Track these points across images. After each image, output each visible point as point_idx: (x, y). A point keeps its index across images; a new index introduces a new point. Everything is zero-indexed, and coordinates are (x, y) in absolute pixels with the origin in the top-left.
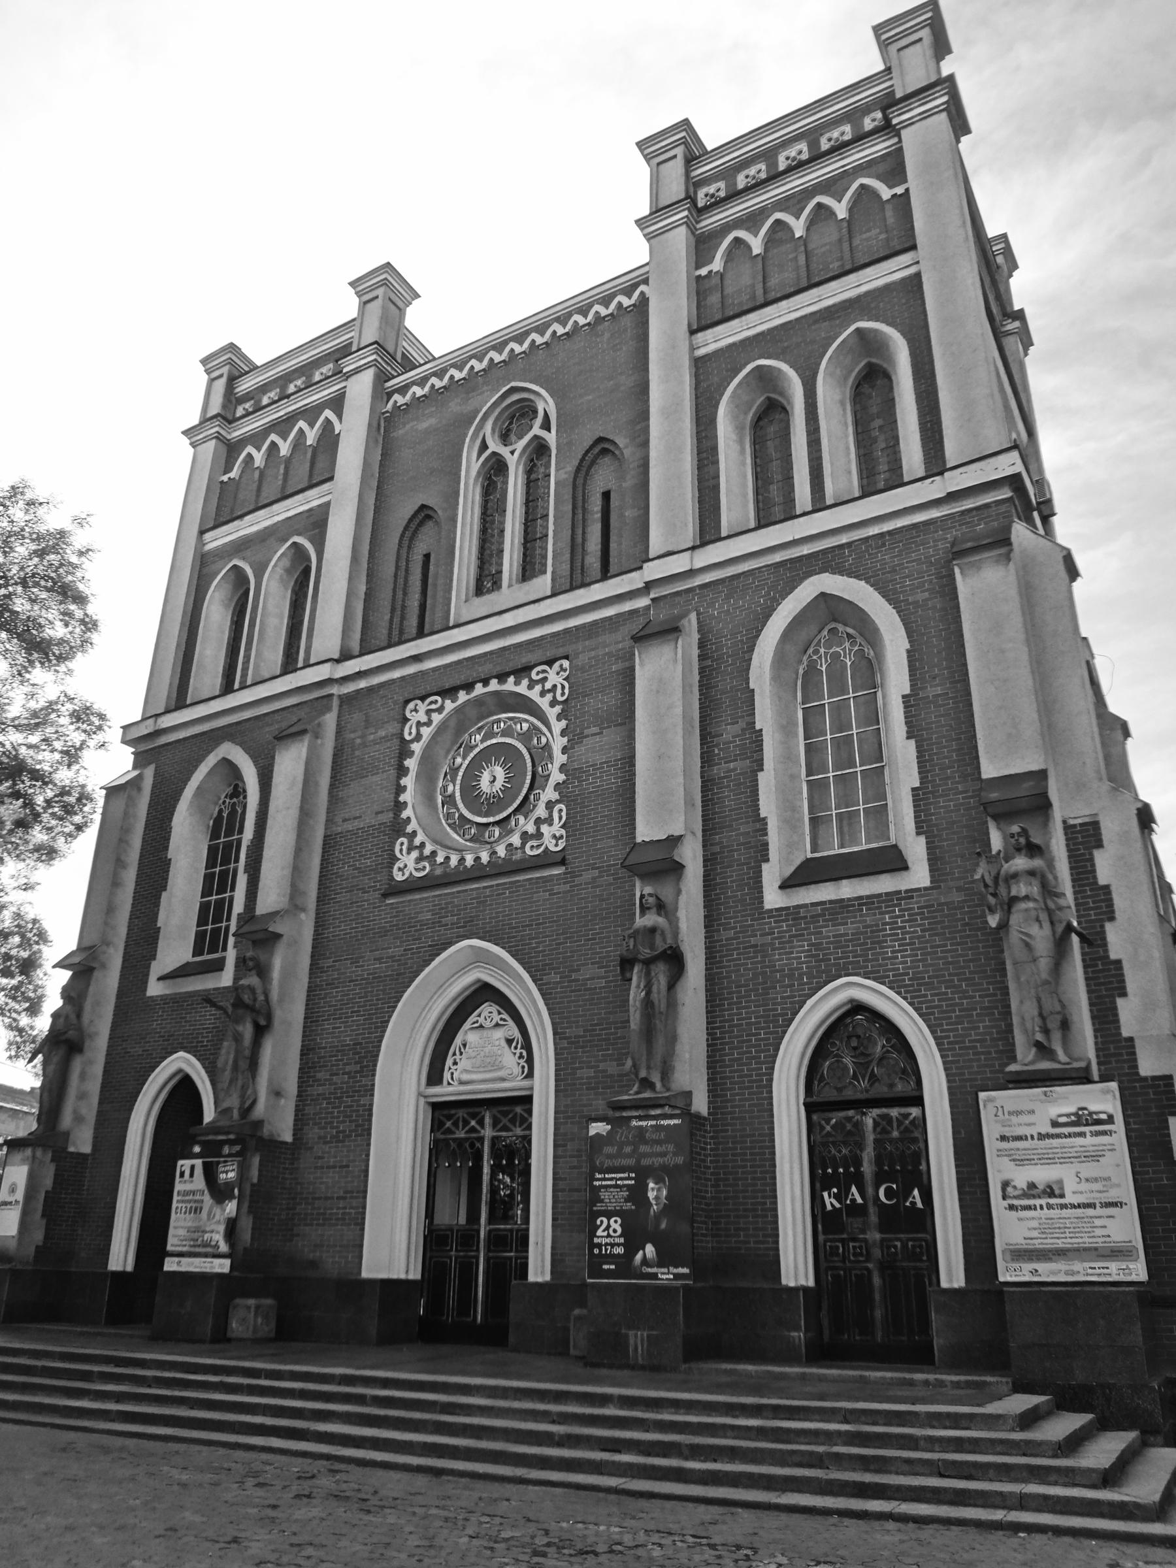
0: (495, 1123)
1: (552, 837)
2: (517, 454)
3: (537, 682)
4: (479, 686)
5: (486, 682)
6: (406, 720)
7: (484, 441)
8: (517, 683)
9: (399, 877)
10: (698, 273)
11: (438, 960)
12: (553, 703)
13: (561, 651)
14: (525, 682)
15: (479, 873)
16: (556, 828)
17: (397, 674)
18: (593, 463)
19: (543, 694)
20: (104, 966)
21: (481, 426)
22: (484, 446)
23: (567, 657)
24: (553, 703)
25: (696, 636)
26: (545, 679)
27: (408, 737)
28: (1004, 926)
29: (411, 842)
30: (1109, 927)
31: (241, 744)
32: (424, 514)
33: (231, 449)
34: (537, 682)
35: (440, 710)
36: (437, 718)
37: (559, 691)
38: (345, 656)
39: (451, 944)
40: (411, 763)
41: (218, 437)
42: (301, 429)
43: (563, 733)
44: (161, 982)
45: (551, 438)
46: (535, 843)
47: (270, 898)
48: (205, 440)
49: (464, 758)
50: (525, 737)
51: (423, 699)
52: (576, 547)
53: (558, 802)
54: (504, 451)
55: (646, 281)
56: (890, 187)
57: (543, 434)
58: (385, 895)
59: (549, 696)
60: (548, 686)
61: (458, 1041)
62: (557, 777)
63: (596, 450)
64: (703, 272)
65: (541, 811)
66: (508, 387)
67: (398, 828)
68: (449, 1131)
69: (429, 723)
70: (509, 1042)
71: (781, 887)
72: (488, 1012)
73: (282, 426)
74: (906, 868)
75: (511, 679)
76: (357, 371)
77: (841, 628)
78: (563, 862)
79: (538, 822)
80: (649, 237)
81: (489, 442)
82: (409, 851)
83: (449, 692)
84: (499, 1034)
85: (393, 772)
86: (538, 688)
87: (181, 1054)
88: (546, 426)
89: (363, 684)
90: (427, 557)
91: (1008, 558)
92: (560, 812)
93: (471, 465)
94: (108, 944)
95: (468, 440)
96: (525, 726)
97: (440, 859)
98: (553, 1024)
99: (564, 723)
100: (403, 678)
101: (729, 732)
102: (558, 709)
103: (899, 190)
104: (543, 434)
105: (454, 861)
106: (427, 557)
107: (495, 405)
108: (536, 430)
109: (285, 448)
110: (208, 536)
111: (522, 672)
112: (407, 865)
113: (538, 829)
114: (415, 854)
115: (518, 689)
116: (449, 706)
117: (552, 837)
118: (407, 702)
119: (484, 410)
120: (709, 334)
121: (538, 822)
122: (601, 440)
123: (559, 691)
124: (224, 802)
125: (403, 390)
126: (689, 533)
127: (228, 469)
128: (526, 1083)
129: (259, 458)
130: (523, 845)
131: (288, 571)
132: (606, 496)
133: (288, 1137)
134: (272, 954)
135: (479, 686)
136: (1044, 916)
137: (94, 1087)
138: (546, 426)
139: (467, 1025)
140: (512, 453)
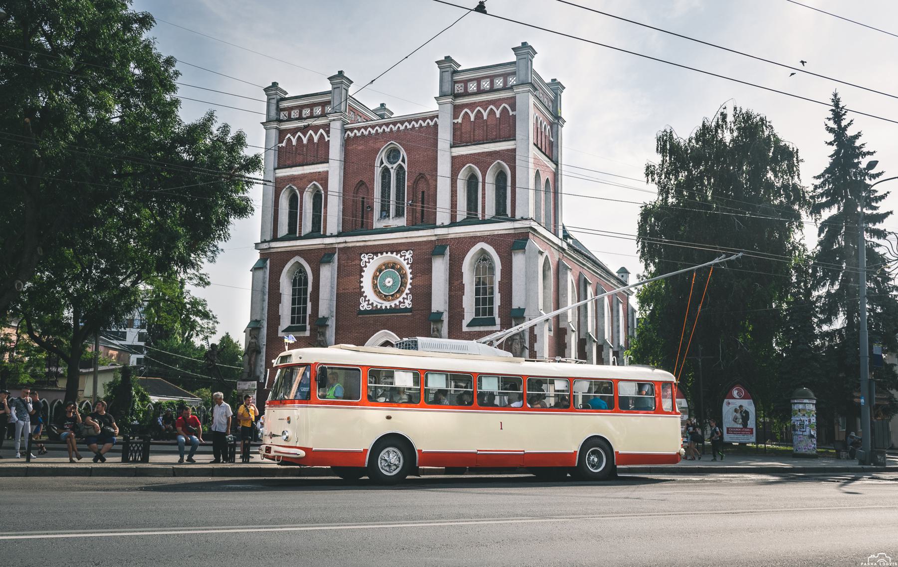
1: (408, 304)
8: (397, 255)
9: (362, 309)
10: (454, 121)
12: (408, 263)
14: (399, 255)
15: (386, 311)
18: (419, 180)
19: (405, 260)
20: (263, 327)
22: (382, 163)
24: (408, 263)
25: (449, 253)
26: (405, 256)
27: (362, 266)
28: (511, 344)
29: (365, 299)
30: (535, 344)
32: (362, 183)
33: (282, 134)
38: (339, 235)
39: (379, 331)
41: (277, 128)
43: (411, 273)
45: (405, 166)
47: (323, 311)
48: (270, 128)
51: (367, 254)
52: (412, 212)
54: (389, 166)
55: (437, 117)
56: (512, 111)
58: (358, 314)
59: (407, 261)
60: (406, 258)
62: (409, 286)
64: (456, 121)
65: (404, 295)
67: (361, 294)
69: (369, 262)
71: (467, 326)
73: (305, 130)
75: (395, 253)
76: (334, 120)
78: (411, 312)
79: (404, 298)
80: (439, 104)
82: (365, 302)
83: (376, 254)
86: (403, 258)
88: (403, 161)
91: (524, 252)
93: (378, 171)
94: (263, 320)
97: (374, 305)
99: (411, 270)
100: (360, 246)
101: (456, 283)
102: (409, 265)
107: (384, 149)
108: (400, 162)
109: (305, 141)
110: (277, 171)
111: (398, 252)
112: (364, 306)
114: (367, 303)
117: (408, 304)
119: (382, 149)
121: (404, 298)
122: (420, 174)
125: (352, 130)
126: (447, 222)
127: (281, 141)
130: (400, 304)
132: (423, 192)
134: (326, 330)
135: (385, 253)
136: (519, 344)
138: (403, 161)
140: (392, 168)
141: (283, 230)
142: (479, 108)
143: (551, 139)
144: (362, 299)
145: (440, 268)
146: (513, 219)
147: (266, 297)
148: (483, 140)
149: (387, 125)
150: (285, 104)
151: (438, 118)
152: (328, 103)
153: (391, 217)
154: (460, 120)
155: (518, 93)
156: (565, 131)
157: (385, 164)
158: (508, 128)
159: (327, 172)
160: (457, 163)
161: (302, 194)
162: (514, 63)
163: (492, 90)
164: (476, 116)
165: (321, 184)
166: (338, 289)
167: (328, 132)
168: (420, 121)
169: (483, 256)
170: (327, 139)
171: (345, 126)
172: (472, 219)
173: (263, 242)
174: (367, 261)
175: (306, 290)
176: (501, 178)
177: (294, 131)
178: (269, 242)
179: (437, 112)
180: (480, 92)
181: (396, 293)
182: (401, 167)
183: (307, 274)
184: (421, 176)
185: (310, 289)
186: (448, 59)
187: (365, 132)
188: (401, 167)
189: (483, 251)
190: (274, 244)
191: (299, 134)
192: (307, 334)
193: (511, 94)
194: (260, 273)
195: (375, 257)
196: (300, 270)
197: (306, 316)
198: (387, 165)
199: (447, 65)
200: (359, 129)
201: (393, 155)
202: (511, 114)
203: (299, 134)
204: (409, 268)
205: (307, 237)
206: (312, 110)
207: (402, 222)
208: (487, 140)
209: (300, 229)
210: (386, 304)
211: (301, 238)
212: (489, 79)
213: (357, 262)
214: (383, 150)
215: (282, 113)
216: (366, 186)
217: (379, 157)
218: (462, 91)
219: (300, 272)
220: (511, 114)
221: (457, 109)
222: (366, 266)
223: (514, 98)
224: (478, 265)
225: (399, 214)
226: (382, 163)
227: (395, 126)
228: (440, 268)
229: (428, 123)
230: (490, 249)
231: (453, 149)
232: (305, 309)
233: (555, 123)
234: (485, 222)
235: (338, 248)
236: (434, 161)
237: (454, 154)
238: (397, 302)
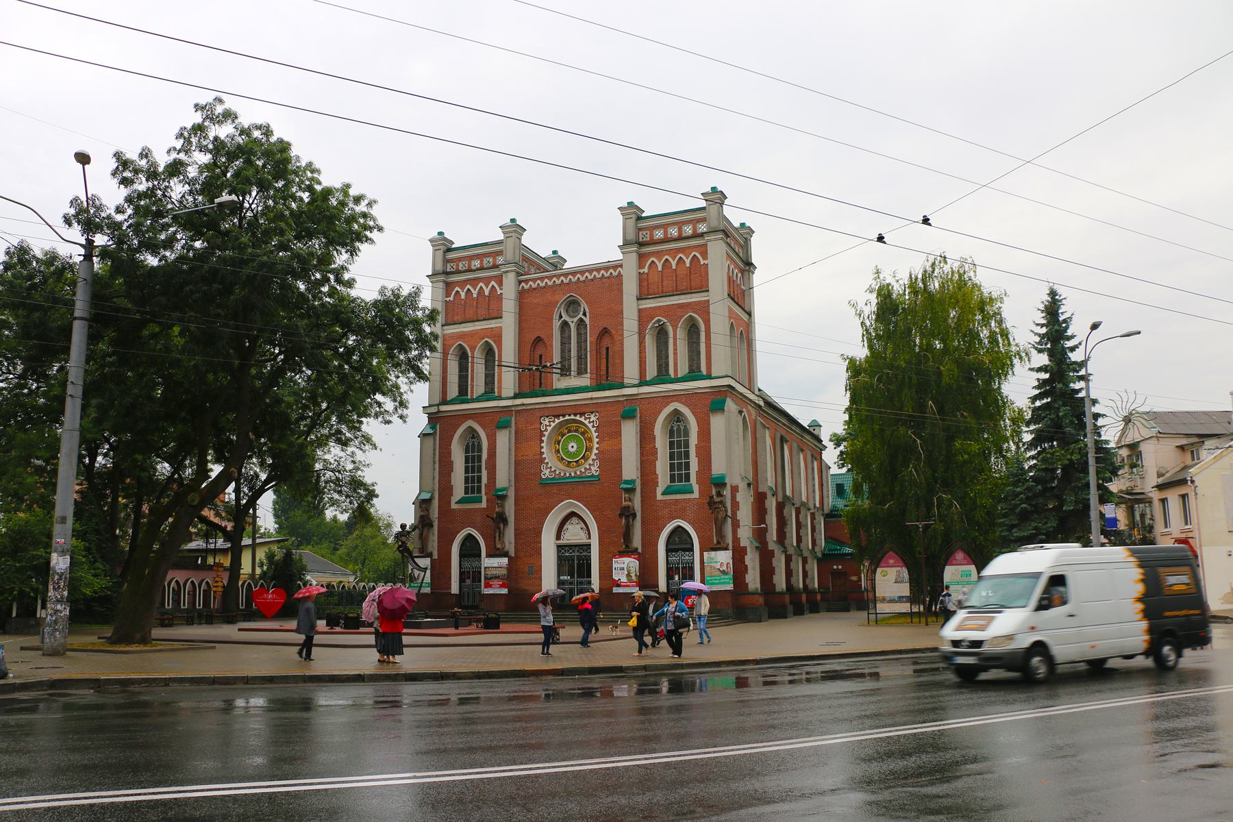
0: (578, 551)
4: (567, 416)
5: (570, 415)
11: (559, 505)
12: (593, 426)
13: (595, 410)
18: (603, 335)
19: (590, 422)
21: (559, 308)
22: (561, 317)
24: (593, 426)
25: (639, 415)
26: (590, 418)
30: (738, 512)
31: (477, 422)
32: (538, 340)
33: (449, 286)
35: (554, 421)
36: (553, 425)
38: (516, 396)
40: (544, 439)
41: (444, 281)
42: (481, 287)
43: (597, 437)
44: (456, 505)
45: (587, 320)
46: (589, 471)
49: (562, 438)
50: (583, 434)
51: (547, 417)
52: (598, 368)
55: (621, 266)
57: (583, 317)
61: (565, 527)
64: (642, 271)
67: (542, 460)
68: (563, 553)
69: (550, 426)
70: (582, 529)
71: (662, 494)
72: (575, 520)
73: (474, 282)
75: (578, 416)
81: (563, 315)
83: (558, 416)
84: (579, 526)
86: (588, 420)
88: (585, 314)
89: (524, 407)
90: (541, 356)
93: (557, 324)
96: (583, 430)
97: (557, 472)
98: (598, 527)
102: (595, 428)
103: (706, 262)
104: (583, 317)
105: (562, 474)
106: (541, 356)
108: (581, 315)
110: (445, 328)
111: (582, 414)
112: (546, 473)
114: (549, 470)
115: (580, 419)
116: (557, 421)
117: (595, 470)
120: (643, 302)
122: (606, 328)
125: (526, 281)
127: (448, 295)
128: (588, 541)
129: (463, 295)
130: (585, 472)
131: (484, 350)
132: (607, 348)
133: (513, 555)
135: (567, 416)
137: (436, 538)
138: (585, 314)
139: (568, 523)
140: (572, 322)
141: (453, 391)
142: (667, 257)
143: (743, 287)
145: (629, 433)
146: (709, 377)
147: (437, 466)
148: (673, 292)
149: (558, 276)
150: (451, 256)
151: (622, 268)
152: (500, 253)
153: (572, 373)
154: (646, 270)
155: (710, 241)
156: (757, 278)
158: (700, 278)
159: (501, 327)
160: (644, 317)
161: (473, 349)
162: (704, 209)
163: (680, 238)
164: (663, 265)
165: (494, 342)
166: (516, 456)
167: (500, 284)
168: (602, 272)
169: (677, 416)
170: (499, 292)
171: (519, 278)
172: (663, 375)
173: (430, 406)
175: (480, 457)
177: (462, 284)
178: (438, 405)
179: (621, 261)
180: (666, 240)
181: (581, 459)
182: (581, 320)
183: (481, 439)
184: (605, 332)
185: (485, 456)
186: (631, 204)
187: (541, 285)
188: (581, 320)
189: (676, 412)
190: (443, 408)
191: (468, 286)
194: (430, 441)
196: (473, 435)
197: (481, 486)
198: (566, 319)
199: (632, 212)
200: (534, 280)
201: (572, 305)
202: (702, 263)
203: (468, 286)
204: (595, 432)
205: (478, 400)
206: (482, 261)
207: (585, 381)
208: (676, 291)
209: (472, 390)
210: (570, 472)
211: (472, 401)
212: (677, 227)
213: (537, 426)
215: (448, 265)
216: (544, 342)
217: (557, 312)
218: (648, 239)
219: (473, 437)
220: (702, 263)
221: (642, 258)
222: (546, 430)
223: (705, 246)
224: (672, 427)
225: (581, 371)
227: (574, 277)
228: (629, 433)
230: (685, 410)
231: (640, 302)
232: (479, 480)
233: (746, 270)
234: (678, 380)
236: (618, 314)
237: (641, 307)
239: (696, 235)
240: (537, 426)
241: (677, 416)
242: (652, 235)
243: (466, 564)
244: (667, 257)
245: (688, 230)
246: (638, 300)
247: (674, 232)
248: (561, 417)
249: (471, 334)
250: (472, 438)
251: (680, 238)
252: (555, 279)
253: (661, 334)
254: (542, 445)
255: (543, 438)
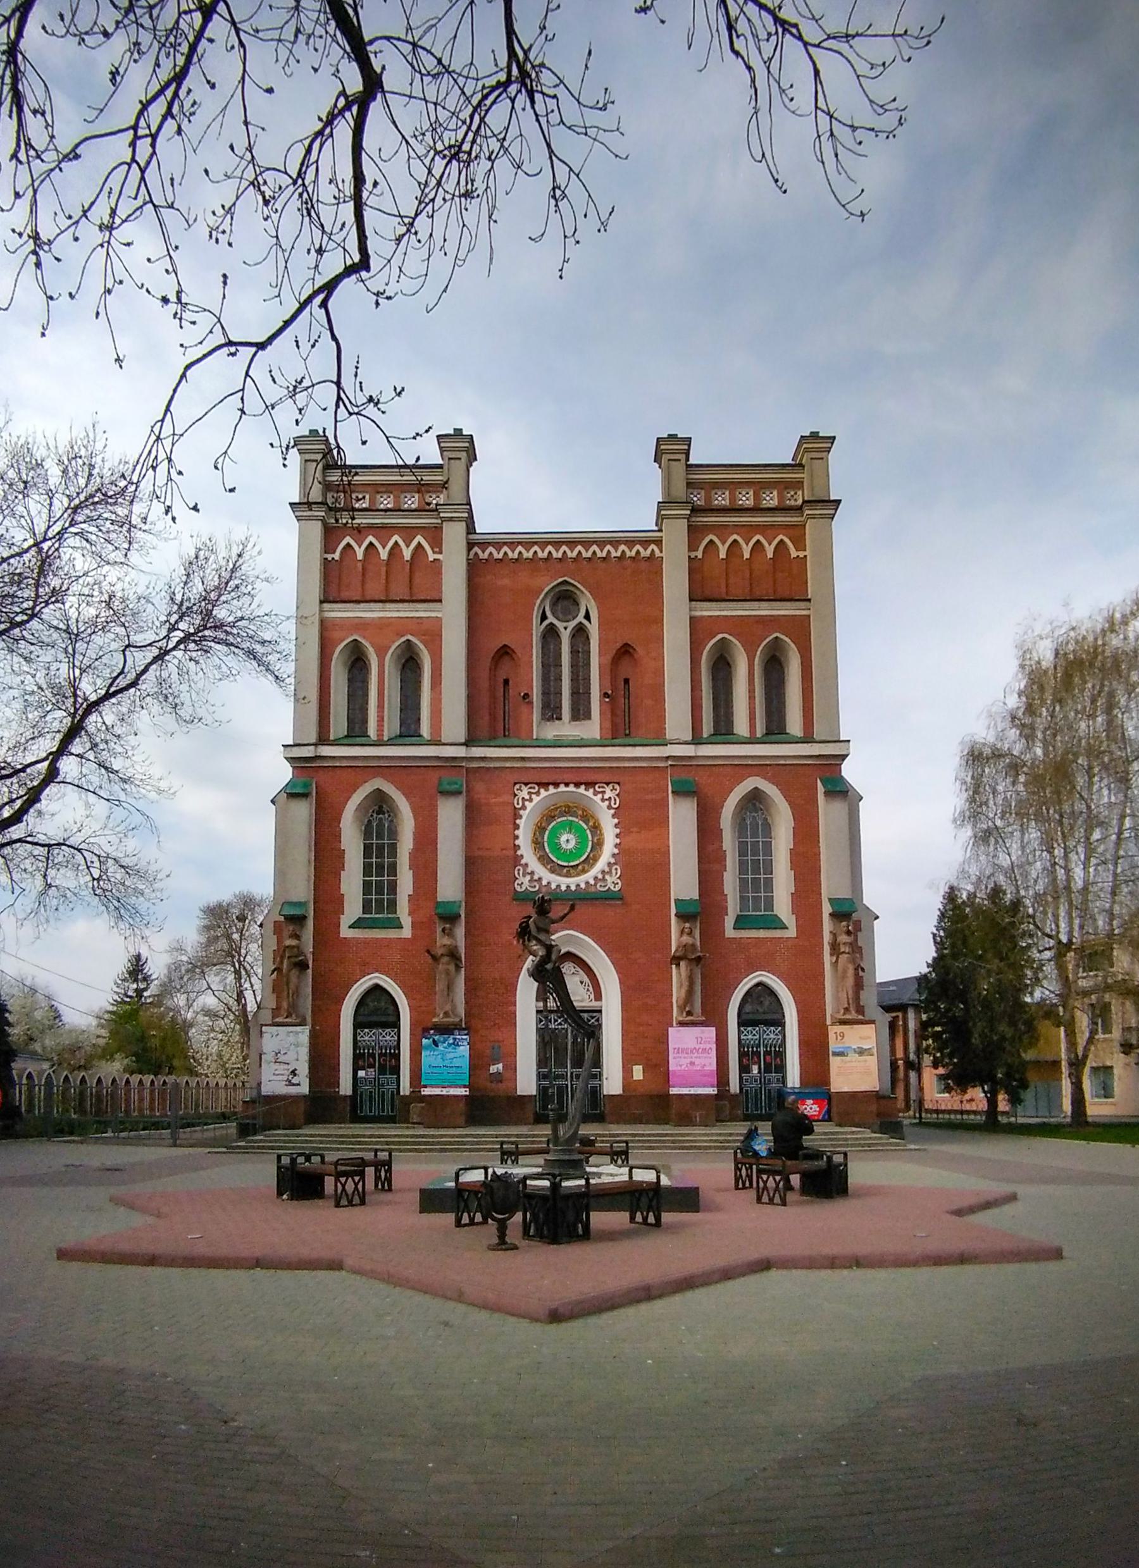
1: (613, 883)
2: (569, 630)
3: (599, 792)
5: (567, 785)
6: (516, 795)
7: (544, 613)
9: (518, 889)
12: (609, 807)
14: (591, 790)
16: (615, 879)
17: (508, 765)
19: (603, 800)
22: (544, 617)
23: (618, 783)
24: (609, 807)
26: (604, 792)
27: (517, 806)
29: (524, 870)
34: (599, 792)
35: (538, 793)
37: (613, 802)
45: (593, 629)
51: (526, 784)
53: (615, 864)
54: (560, 625)
59: (607, 803)
60: (606, 796)
63: (623, 650)
64: (693, 555)
66: (560, 580)
67: (517, 860)
69: (531, 800)
74: (787, 928)
75: (583, 787)
77: (757, 804)
81: (548, 613)
83: (545, 785)
85: (511, 826)
86: (600, 796)
87: (377, 974)
89: (482, 764)
92: (618, 871)
93: (537, 629)
95: (536, 608)
97: (544, 883)
102: (612, 811)
104: (585, 622)
108: (580, 618)
111: (589, 785)
113: (604, 877)
114: (528, 877)
116: (543, 793)
118: (515, 784)
119: (546, 590)
122: (626, 644)
123: (613, 802)
124: (372, 816)
130: (595, 884)
131: (399, 657)
138: (587, 617)
140: (566, 628)
142: (735, 537)
144: (518, 871)
146: (808, 739)
154: (699, 554)
157: (551, 619)
163: (757, 509)
170: (431, 557)
174: (527, 797)
176: (774, 666)
184: (625, 651)
192: (407, 932)
193: (799, 519)
195: (542, 791)
196: (381, 807)
198: (555, 622)
204: (614, 816)
211: (379, 743)
213: (506, 798)
214: (547, 593)
217: (540, 605)
219: (380, 811)
221: (695, 533)
222: (524, 807)
225: (580, 713)
226: (544, 617)
229: (638, 552)
235: (467, 769)
238: (589, 876)
239: (781, 509)
240: (506, 798)
241: (755, 798)
242: (708, 499)
243: (368, 1037)
244: (735, 537)
245: (771, 499)
246: (691, 600)
247: (746, 499)
248: (551, 787)
249: (382, 625)
250: (378, 814)
251: (757, 509)
252: (536, 548)
253: (722, 666)
254: (517, 832)
255: (518, 821)
